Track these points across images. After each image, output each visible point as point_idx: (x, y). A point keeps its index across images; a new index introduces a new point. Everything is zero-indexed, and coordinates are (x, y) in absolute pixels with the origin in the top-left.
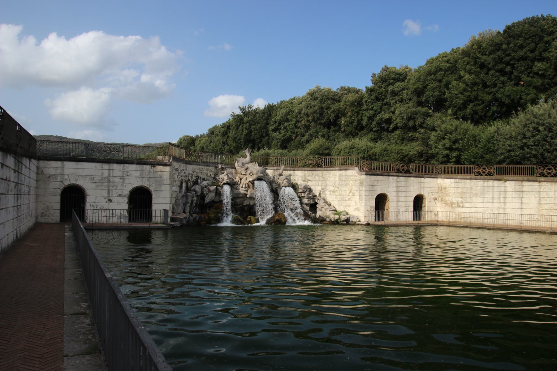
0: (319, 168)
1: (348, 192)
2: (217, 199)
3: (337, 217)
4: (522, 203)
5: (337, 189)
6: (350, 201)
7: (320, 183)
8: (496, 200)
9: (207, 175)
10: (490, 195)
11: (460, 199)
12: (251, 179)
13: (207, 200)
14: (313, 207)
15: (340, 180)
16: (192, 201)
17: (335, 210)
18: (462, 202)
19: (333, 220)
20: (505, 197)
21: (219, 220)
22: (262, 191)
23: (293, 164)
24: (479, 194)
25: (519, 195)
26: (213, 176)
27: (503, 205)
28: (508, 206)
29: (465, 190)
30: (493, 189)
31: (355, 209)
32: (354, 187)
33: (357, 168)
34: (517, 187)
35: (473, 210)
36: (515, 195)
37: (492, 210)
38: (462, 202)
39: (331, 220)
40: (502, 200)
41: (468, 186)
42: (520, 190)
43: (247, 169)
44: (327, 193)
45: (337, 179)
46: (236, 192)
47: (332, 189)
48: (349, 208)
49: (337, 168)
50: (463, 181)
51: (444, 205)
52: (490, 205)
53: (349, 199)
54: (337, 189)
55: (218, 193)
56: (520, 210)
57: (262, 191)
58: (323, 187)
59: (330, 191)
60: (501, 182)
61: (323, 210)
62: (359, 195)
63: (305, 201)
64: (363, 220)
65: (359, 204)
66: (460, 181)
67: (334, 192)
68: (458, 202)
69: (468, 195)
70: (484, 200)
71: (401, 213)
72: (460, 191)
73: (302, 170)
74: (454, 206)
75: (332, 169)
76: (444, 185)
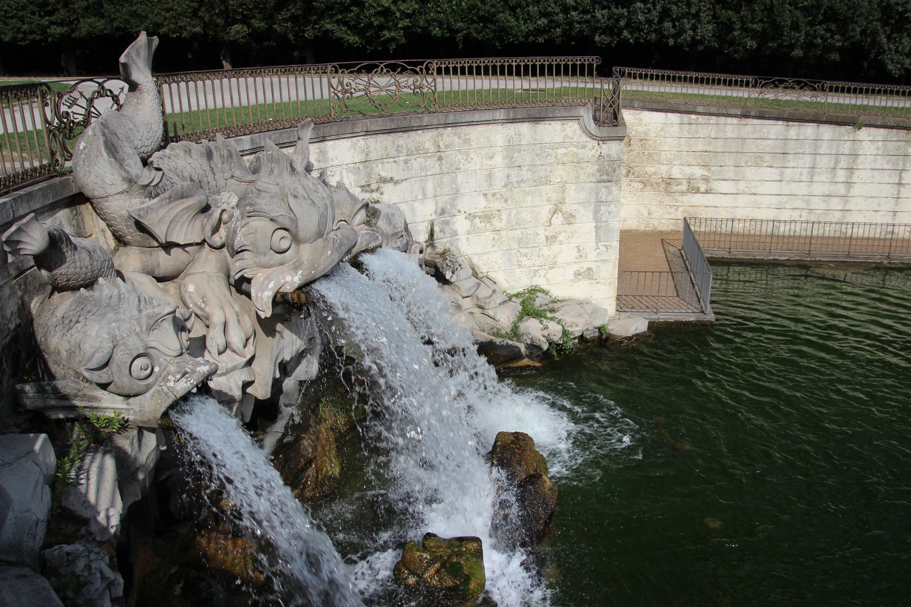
0: (426, 120)
1: (545, 211)
3: (555, 331)
4: (900, 184)
5: (497, 205)
6: (556, 247)
7: (430, 186)
8: (824, 177)
10: (807, 161)
11: (698, 172)
12: (291, 281)
15: (512, 164)
18: (706, 179)
19: (545, 347)
20: (851, 170)
24: (767, 157)
25: (897, 164)
27: (841, 189)
28: (856, 190)
29: (720, 146)
30: (816, 148)
31: (578, 274)
32: (571, 190)
33: (586, 114)
34: (891, 145)
35: (743, 200)
36: (881, 163)
37: (808, 202)
38: (706, 179)
39: (533, 347)
40: (841, 175)
41: (729, 135)
42: (901, 152)
44: (461, 224)
45: (498, 160)
47: (480, 204)
48: (552, 274)
49: (500, 114)
50: (713, 119)
51: (640, 186)
52: (802, 189)
53: (551, 240)
54: (497, 205)
56: (893, 201)
58: (443, 201)
59: (471, 217)
60: (843, 129)
61: (467, 303)
62: (596, 219)
65: (592, 256)
66: (701, 119)
67: (487, 217)
68: (689, 180)
69: (729, 160)
70: (782, 174)
72: (700, 147)
73: (354, 135)
74: (675, 188)
75: (477, 117)
76: (641, 129)
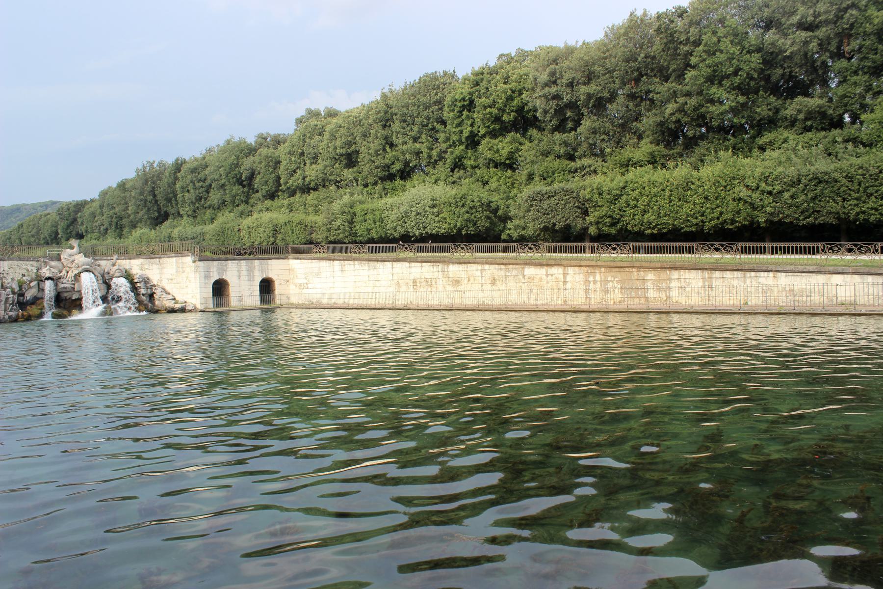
2: (40, 295)
9: (28, 270)
13: (29, 295)
14: (151, 296)
16: (7, 299)
17: (174, 299)
21: (41, 315)
22: (88, 283)
23: (124, 253)
26: (35, 271)
43: (73, 262)
46: (61, 286)
55: (41, 290)
57: (88, 283)
63: (142, 291)
64: (199, 307)
71: (244, 298)
